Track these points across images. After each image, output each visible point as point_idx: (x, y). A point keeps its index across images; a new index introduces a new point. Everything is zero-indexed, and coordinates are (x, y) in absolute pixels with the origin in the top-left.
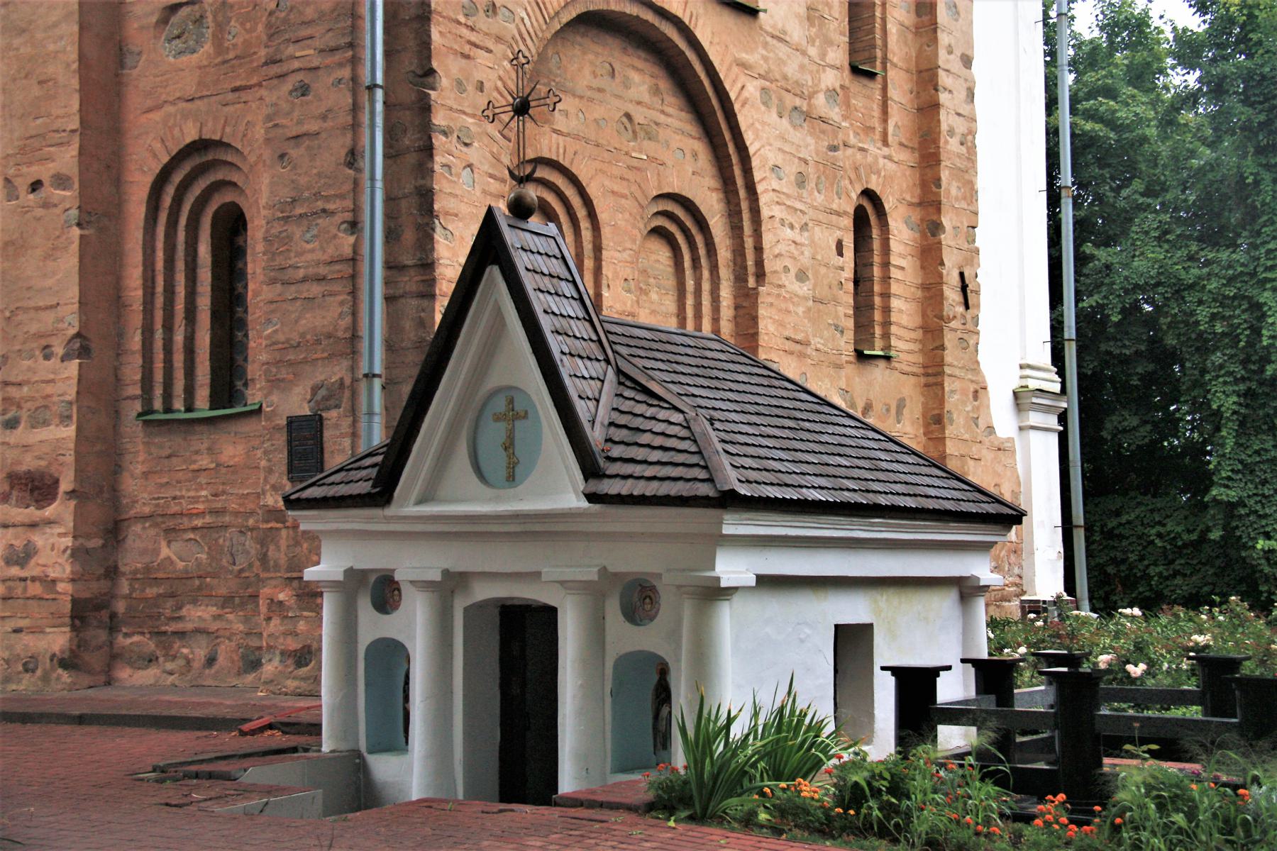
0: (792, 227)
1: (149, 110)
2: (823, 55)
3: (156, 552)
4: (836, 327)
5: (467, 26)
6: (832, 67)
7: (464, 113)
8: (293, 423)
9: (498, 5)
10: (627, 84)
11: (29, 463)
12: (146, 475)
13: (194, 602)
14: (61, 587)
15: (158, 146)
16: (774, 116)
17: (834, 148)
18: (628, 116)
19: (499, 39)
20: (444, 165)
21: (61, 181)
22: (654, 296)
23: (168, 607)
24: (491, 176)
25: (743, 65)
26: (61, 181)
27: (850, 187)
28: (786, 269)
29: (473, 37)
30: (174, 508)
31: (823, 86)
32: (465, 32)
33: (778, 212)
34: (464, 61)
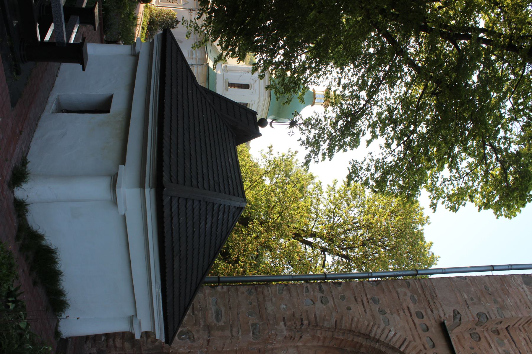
5: (367, 299)
7: (333, 300)
9: (386, 315)
19: (373, 317)
20: (307, 288)
24: (315, 315)
34: (353, 299)
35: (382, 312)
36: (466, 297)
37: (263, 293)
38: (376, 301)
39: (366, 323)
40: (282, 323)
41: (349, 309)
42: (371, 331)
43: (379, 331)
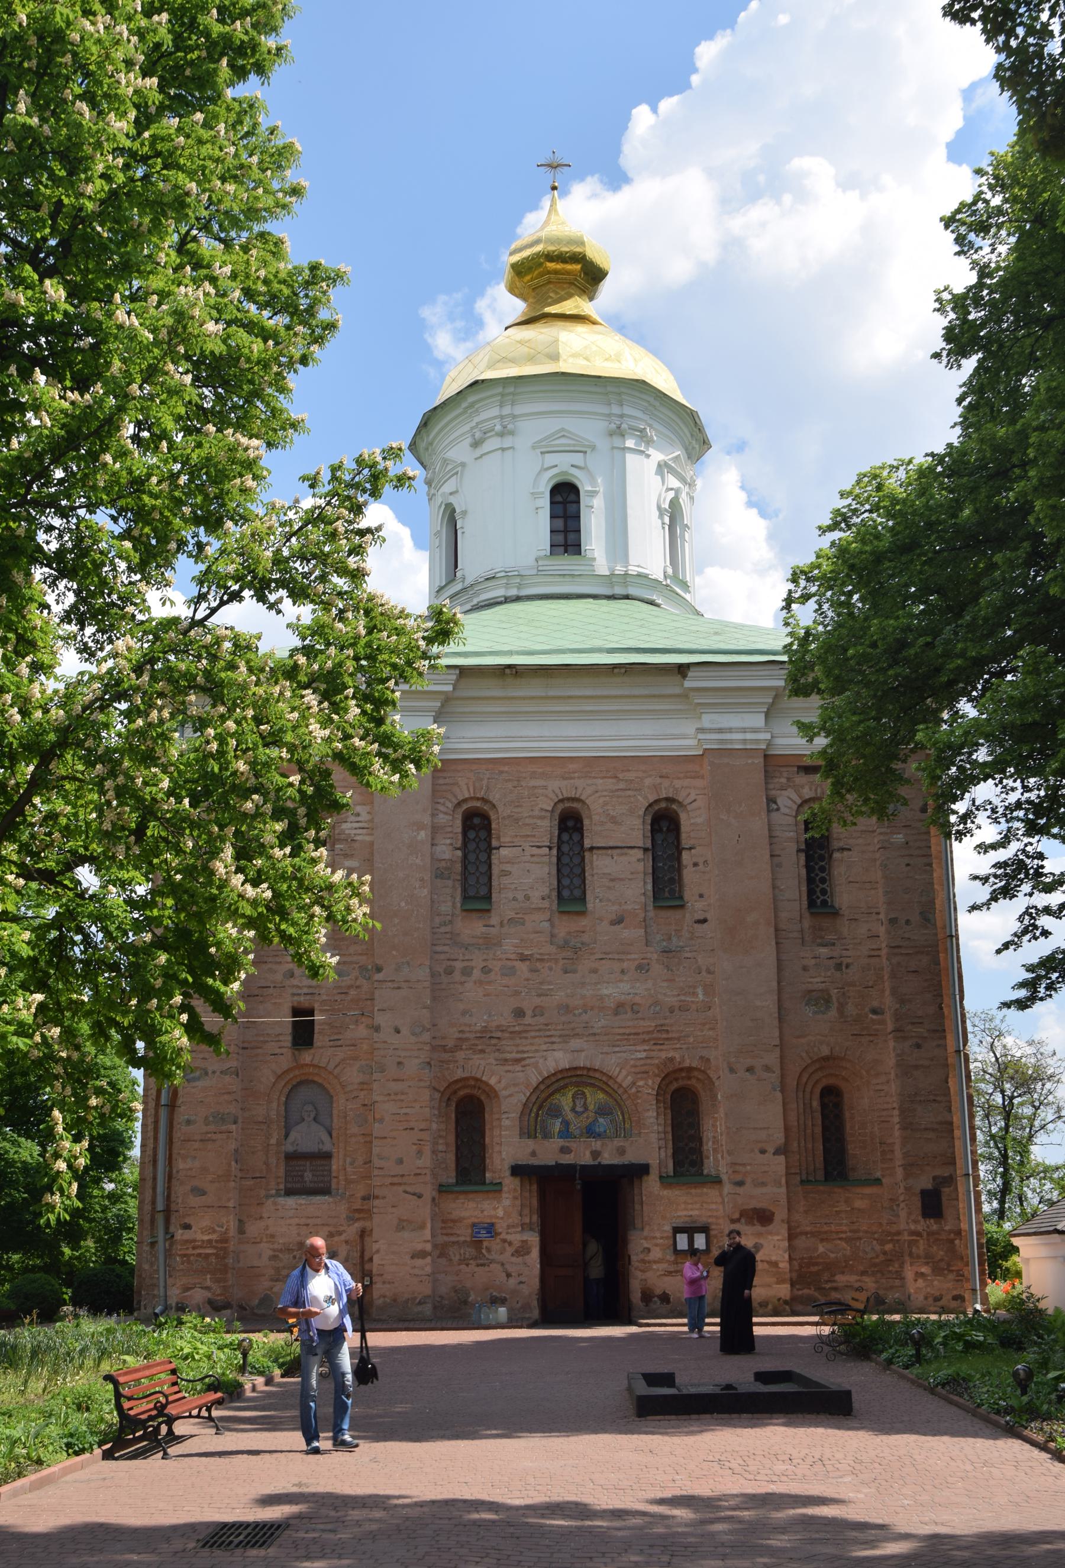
1: (798, 1037)
3: (816, 1249)
8: (924, 1193)
11: (754, 1204)
12: (806, 1212)
13: (843, 1273)
14: (781, 1265)
15: (804, 1055)
21: (767, 1068)
23: (826, 1276)
26: (767, 1068)
30: (826, 1228)
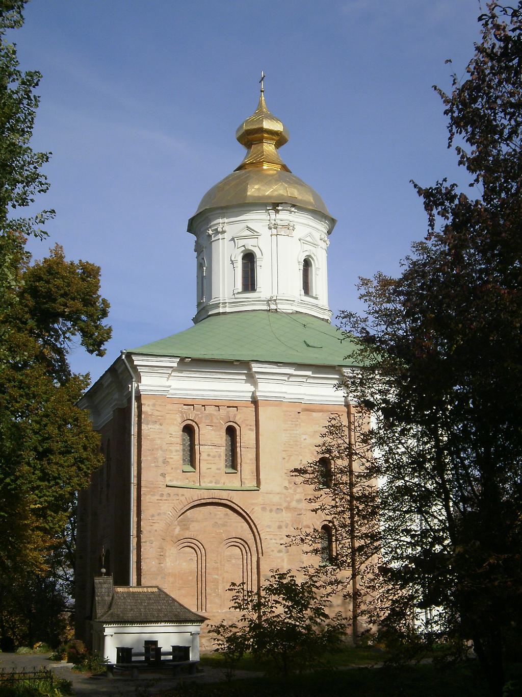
0: (275, 539)
2: (295, 491)
4: (301, 562)
6: (299, 493)
10: (215, 515)
16: (268, 513)
17: (300, 515)
18: (216, 523)
20: (144, 549)
22: (233, 561)
25: (253, 504)
27: (317, 521)
28: (273, 551)
29: (154, 521)
31: (295, 499)
32: (151, 521)
33: (268, 537)
35: (159, 514)
36: (153, 465)
37: (146, 572)
38: (153, 516)
39: (164, 524)
40: (162, 565)
41: (156, 531)
42: (168, 524)
43: (169, 519)
